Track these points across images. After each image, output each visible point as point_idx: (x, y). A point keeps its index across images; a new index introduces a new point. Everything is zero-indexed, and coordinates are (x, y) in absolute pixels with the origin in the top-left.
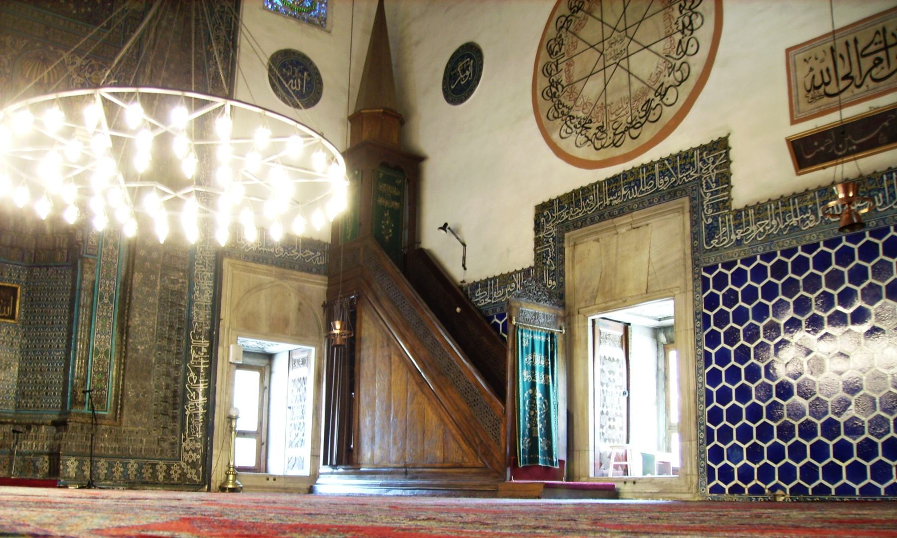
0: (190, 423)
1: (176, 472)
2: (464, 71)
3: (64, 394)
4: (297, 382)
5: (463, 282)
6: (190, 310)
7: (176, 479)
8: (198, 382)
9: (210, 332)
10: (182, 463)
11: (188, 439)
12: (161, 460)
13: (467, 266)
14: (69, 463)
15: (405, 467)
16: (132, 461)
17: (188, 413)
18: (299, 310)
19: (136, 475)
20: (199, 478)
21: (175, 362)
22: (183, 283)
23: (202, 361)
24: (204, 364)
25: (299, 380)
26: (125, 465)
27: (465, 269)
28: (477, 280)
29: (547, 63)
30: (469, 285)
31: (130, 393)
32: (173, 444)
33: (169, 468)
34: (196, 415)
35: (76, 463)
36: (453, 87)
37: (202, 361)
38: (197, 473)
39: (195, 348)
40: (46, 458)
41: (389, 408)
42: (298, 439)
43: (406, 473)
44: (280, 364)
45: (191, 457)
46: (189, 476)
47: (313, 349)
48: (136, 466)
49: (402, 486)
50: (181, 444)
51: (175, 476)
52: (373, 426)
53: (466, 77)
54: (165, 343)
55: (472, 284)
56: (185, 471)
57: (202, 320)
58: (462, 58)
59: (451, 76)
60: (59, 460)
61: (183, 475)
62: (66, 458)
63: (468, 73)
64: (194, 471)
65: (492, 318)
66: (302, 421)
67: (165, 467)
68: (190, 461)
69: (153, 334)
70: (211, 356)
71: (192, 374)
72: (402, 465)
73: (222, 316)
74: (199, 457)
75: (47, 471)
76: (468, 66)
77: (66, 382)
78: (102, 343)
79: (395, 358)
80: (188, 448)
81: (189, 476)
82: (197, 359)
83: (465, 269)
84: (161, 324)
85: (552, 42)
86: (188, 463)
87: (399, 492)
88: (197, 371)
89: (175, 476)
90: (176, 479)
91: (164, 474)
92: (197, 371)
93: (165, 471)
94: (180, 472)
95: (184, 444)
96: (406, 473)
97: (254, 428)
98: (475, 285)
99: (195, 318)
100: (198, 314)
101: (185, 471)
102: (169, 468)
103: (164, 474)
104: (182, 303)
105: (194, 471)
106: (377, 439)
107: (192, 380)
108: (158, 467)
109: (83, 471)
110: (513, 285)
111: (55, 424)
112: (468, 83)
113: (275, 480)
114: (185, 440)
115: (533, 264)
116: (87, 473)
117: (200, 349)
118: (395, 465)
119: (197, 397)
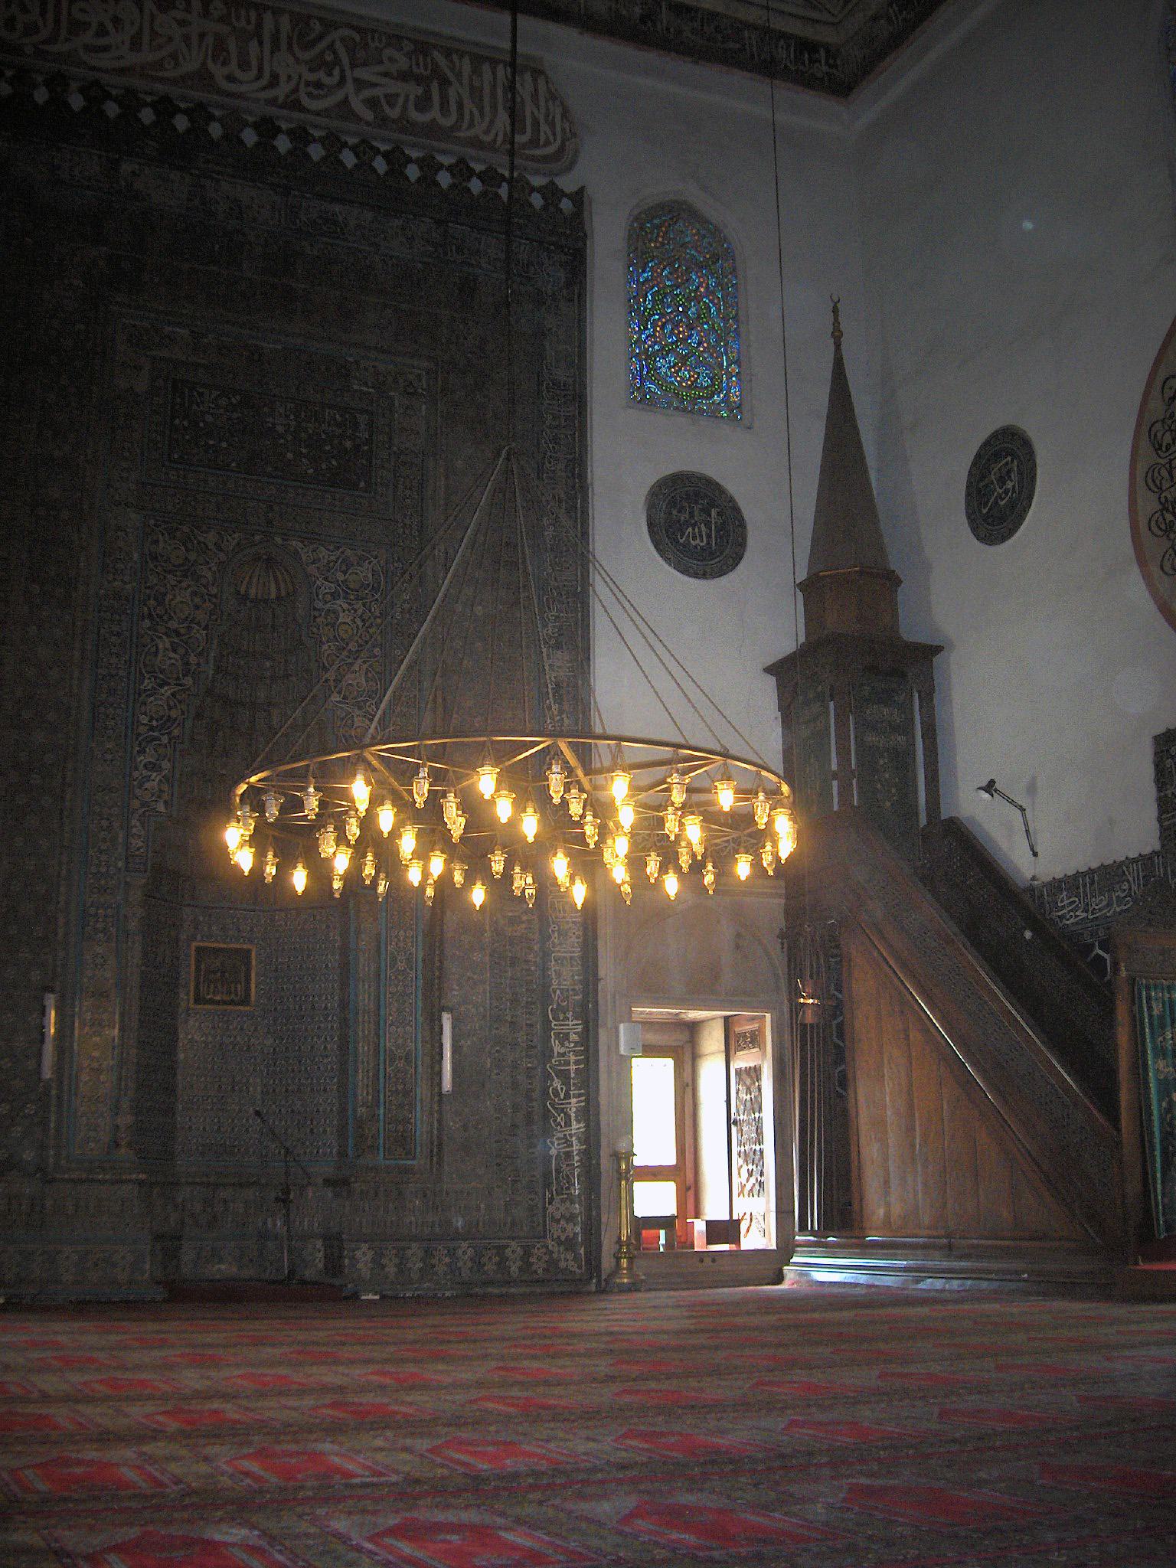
0: (558, 1172)
1: (539, 1259)
2: (1002, 481)
3: (342, 1132)
4: (744, 1076)
5: (1034, 878)
6: (545, 969)
7: (540, 1271)
8: (567, 1096)
9: (584, 1006)
10: (550, 1243)
11: (557, 1199)
12: (513, 1239)
13: (1038, 849)
14: (358, 1254)
15: (948, 1236)
16: (464, 1244)
18: (738, 947)
19: (471, 1269)
20: (580, 1267)
21: (526, 1063)
22: (529, 921)
23: (572, 1058)
24: (577, 1063)
25: (748, 1071)
26: (452, 1253)
27: (1035, 854)
28: (1059, 876)
29: (1152, 468)
30: (1044, 885)
33: (527, 1253)
34: (569, 1155)
35: (370, 1254)
36: (984, 511)
37: (572, 1058)
38: (576, 1258)
39: (557, 1035)
40: (319, 1244)
41: (910, 1129)
42: (752, 1180)
43: (950, 1247)
44: (713, 1041)
45: (564, 1230)
46: (563, 1264)
47: (768, 1016)
48: (470, 1252)
49: (943, 1271)
50: (545, 1209)
51: (539, 1267)
52: (886, 1160)
53: (1006, 492)
55: (1049, 884)
57: (567, 984)
58: (997, 456)
59: (979, 491)
60: (341, 1249)
61: (553, 1263)
62: (353, 1245)
63: (1009, 485)
64: (570, 1256)
65: (1091, 947)
66: (758, 1148)
68: (563, 1238)
69: (484, 1017)
70: (587, 1050)
72: (943, 1232)
73: (602, 973)
74: (578, 1229)
75: (321, 1265)
76: (1009, 472)
77: (343, 1110)
79: (915, 1035)
81: (563, 1264)
82: (563, 1055)
83: (1035, 854)
85: (1158, 426)
86: (560, 1243)
87: (939, 1284)
88: (564, 1076)
89: (539, 1267)
90: (540, 1271)
91: (519, 1263)
92: (564, 1076)
94: (546, 1258)
95: (551, 1209)
96: (950, 1247)
97: (670, 1159)
98: (1057, 885)
99: (555, 982)
100: (559, 974)
102: (527, 1253)
103: (519, 1263)
104: (530, 957)
106: (894, 1182)
108: (508, 1251)
109: (383, 1267)
110: (1126, 886)
111: (328, 1182)
112: (1012, 504)
113: (714, 1261)
114: (551, 1200)
115: (1157, 847)
116: (391, 1270)
117: (567, 1036)
118: (930, 1232)
119: (568, 1124)
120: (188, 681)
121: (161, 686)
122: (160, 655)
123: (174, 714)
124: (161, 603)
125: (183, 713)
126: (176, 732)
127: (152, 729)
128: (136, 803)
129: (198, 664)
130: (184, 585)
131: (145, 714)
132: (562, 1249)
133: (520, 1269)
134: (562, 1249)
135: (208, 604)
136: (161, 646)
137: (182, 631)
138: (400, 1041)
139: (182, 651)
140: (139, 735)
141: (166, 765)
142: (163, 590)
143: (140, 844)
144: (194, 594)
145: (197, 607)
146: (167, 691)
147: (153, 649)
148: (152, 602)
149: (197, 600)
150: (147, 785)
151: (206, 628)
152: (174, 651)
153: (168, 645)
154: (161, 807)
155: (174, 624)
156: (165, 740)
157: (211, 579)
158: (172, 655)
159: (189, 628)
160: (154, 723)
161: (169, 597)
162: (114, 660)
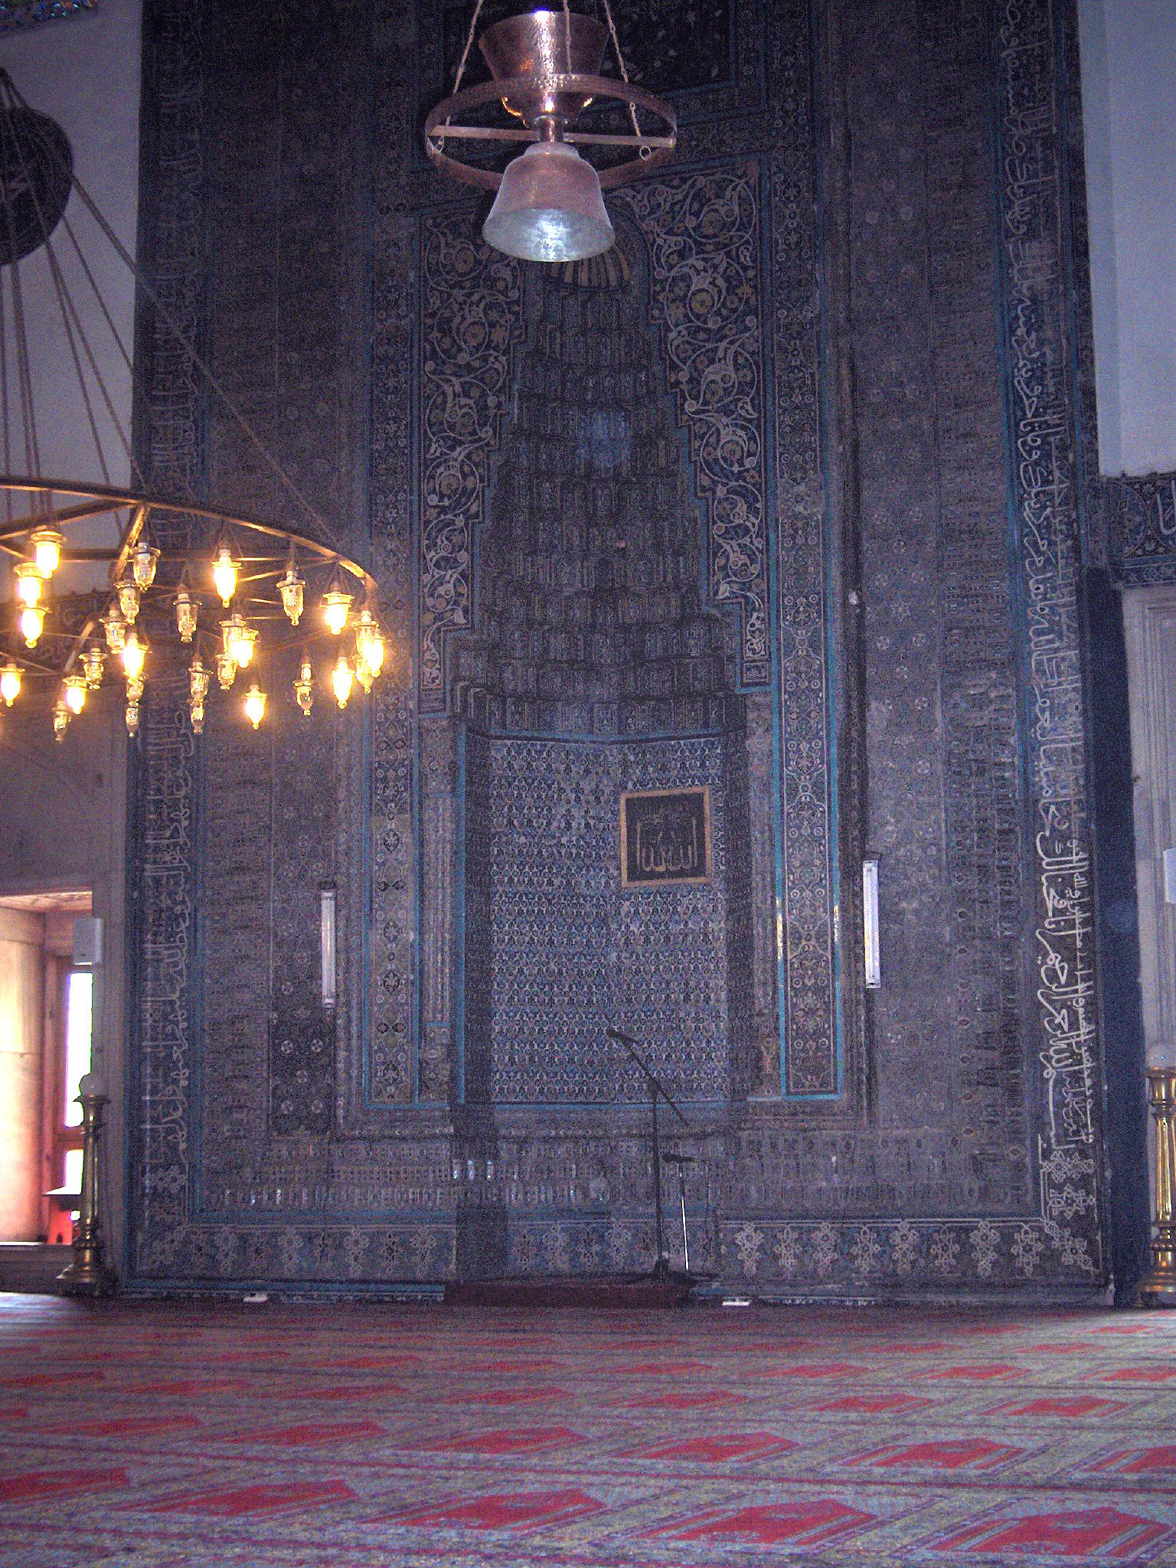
1: (1028, 1249)
7: (1029, 1270)
10: (1045, 1221)
17: (1050, 1073)
20: (1096, 1264)
31: (892, 1036)
32: (1018, 1167)
33: (1007, 1238)
46: (1067, 1259)
50: (1036, 1168)
51: (1027, 1262)
54: (973, 880)
56: (1056, 1244)
61: (1051, 1256)
62: (733, 1224)
67: (994, 1236)
71: (1054, 960)
74: (1093, 1200)
78: (807, 912)
80: (1059, 1177)
81: (1067, 1259)
84: (957, 827)
86: (1063, 1223)
89: (1027, 1262)
90: (1029, 1270)
91: (992, 1256)
93: (997, 1248)
94: (1040, 1247)
95: (1046, 1167)
101: (1056, 1244)
102: (1007, 1238)
103: (992, 1256)
105: (1081, 1245)
107: (1053, 976)
108: (975, 1237)
109: (776, 1257)
117: (1068, 881)
120: (486, 434)
121: (452, 448)
122: (449, 405)
123: (470, 483)
124: (445, 331)
125: (482, 480)
126: (474, 509)
127: (443, 510)
128: (428, 618)
129: (499, 406)
130: (475, 297)
131: (434, 492)
132: (1067, 1232)
133: (994, 1264)
134: (1067, 1232)
135: (508, 316)
136: (449, 391)
137: (477, 364)
138: (807, 912)
139: (475, 392)
140: (427, 523)
141: (463, 557)
142: (447, 313)
143: (435, 673)
144: (489, 307)
145: (492, 325)
146: (459, 453)
147: (440, 400)
148: (435, 334)
149: (494, 315)
150: (441, 590)
151: (505, 352)
152: (467, 395)
153: (458, 389)
154: (459, 618)
155: (463, 358)
156: (460, 522)
157: (509, 278)
158: (464, 401)
159: (485, 359)
160: (446, 502)
161: (457, 320)
162: (392, 428)
